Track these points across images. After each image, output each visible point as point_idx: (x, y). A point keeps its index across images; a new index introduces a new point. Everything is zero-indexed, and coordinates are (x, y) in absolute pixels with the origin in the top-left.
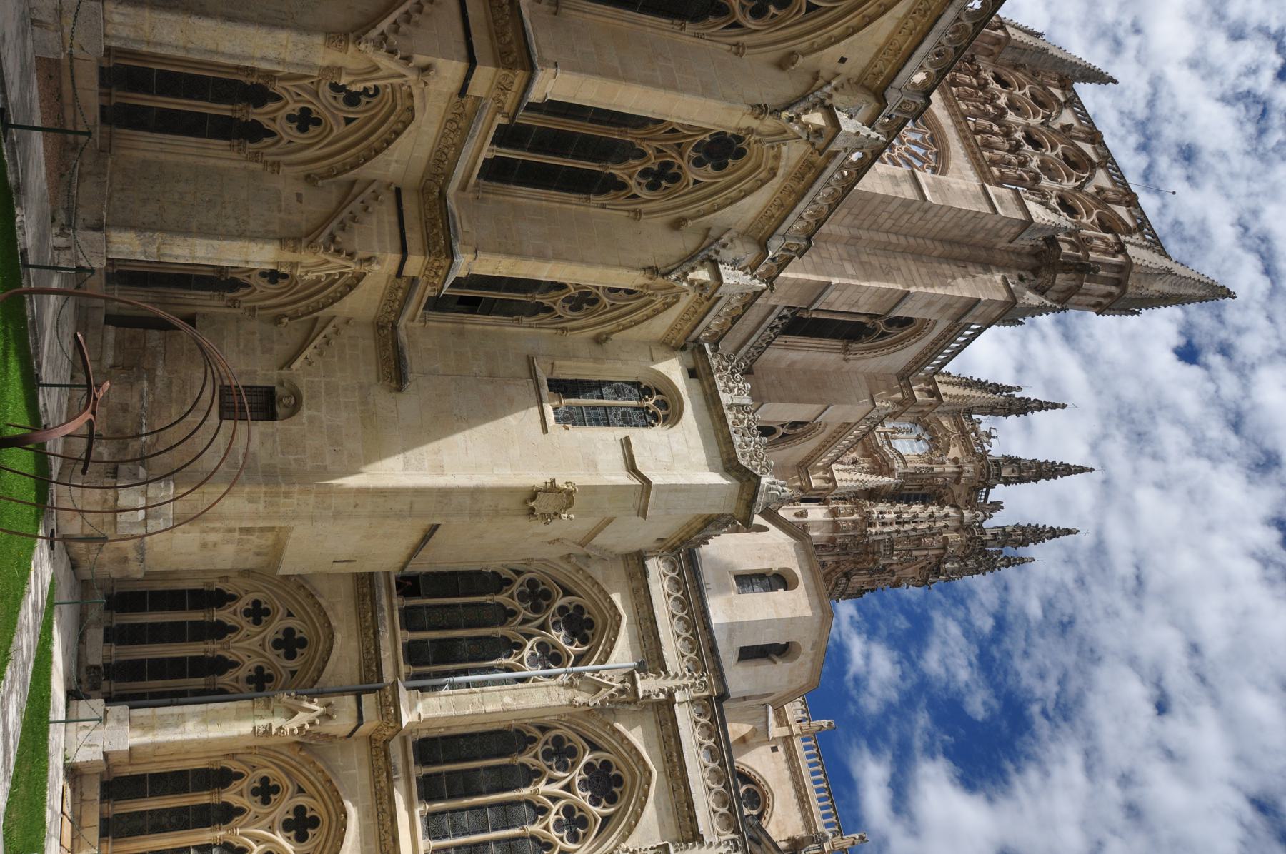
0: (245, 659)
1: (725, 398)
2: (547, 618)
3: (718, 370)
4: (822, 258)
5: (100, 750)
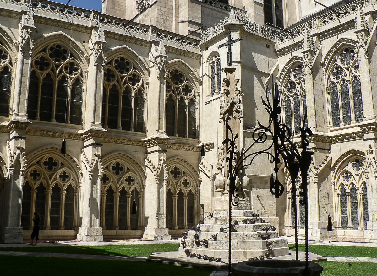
0: (363, 181)
1: (210, 37)
2: (297, 83)
3: (205, 40)
4: (183, 2)
5: (318, 230)
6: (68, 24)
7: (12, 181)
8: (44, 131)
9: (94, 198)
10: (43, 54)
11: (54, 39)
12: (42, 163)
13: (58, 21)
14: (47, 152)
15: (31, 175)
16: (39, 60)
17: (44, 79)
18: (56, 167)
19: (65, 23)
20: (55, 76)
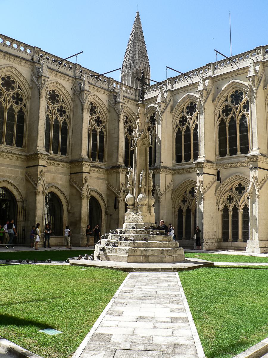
6: (237, 71)
7: (198, 206)
8: (228, 164)
9: (254, 215)
10: (226, 103)
11: (230, 88)
12: (234, 189)
13: (229, 73)
14: (234, 180)
15: (228, 199)
16: (224, 109)
17: (230, 123)
18: (244, 191)
19: (222, 75)
20: (236, 117)
